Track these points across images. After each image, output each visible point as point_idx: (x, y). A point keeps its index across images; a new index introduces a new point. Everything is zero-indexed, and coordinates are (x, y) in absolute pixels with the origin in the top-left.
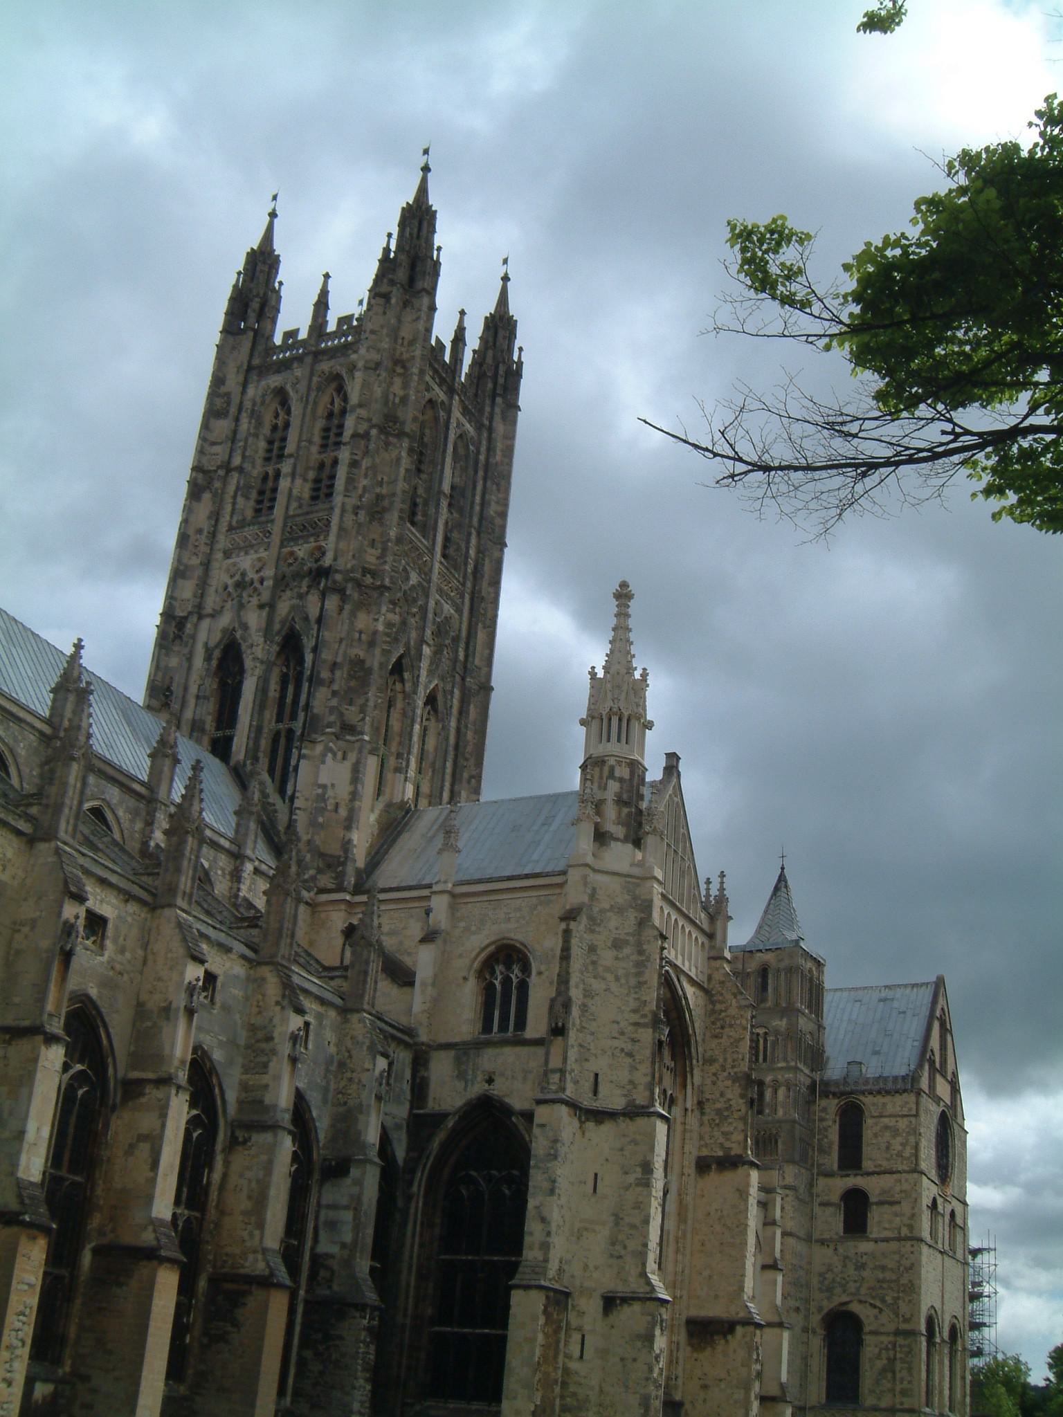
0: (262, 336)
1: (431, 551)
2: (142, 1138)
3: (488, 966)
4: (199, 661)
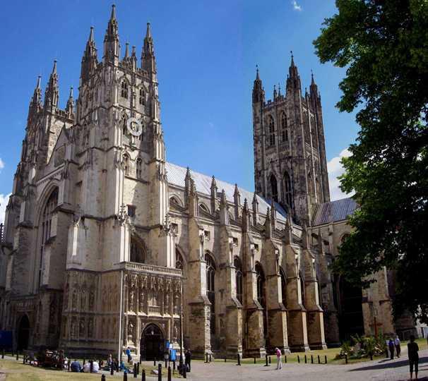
0: (263, 104)
1: (310, 146)
2: (293, 289)
3: (343, 238)
4: (266, 180)
